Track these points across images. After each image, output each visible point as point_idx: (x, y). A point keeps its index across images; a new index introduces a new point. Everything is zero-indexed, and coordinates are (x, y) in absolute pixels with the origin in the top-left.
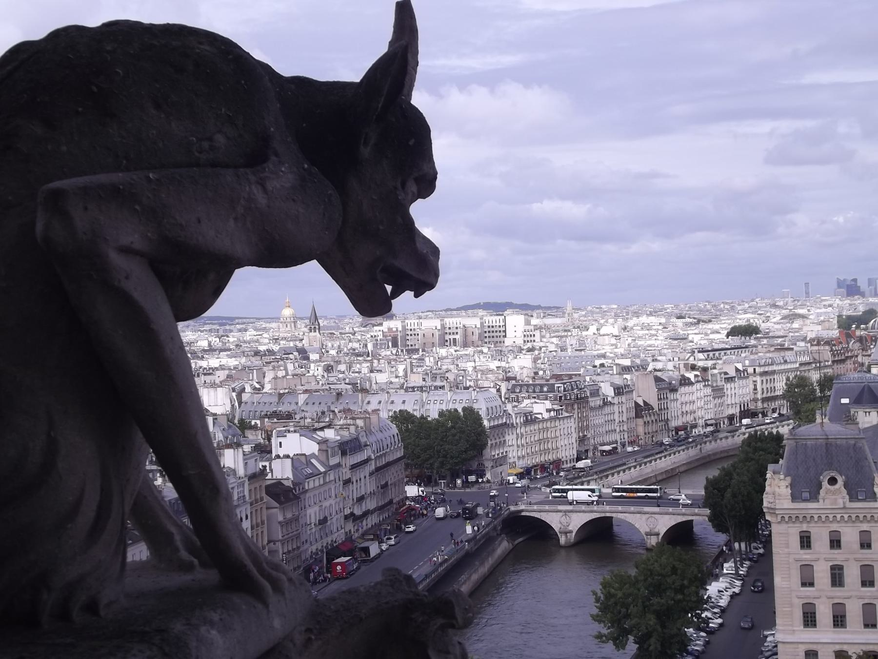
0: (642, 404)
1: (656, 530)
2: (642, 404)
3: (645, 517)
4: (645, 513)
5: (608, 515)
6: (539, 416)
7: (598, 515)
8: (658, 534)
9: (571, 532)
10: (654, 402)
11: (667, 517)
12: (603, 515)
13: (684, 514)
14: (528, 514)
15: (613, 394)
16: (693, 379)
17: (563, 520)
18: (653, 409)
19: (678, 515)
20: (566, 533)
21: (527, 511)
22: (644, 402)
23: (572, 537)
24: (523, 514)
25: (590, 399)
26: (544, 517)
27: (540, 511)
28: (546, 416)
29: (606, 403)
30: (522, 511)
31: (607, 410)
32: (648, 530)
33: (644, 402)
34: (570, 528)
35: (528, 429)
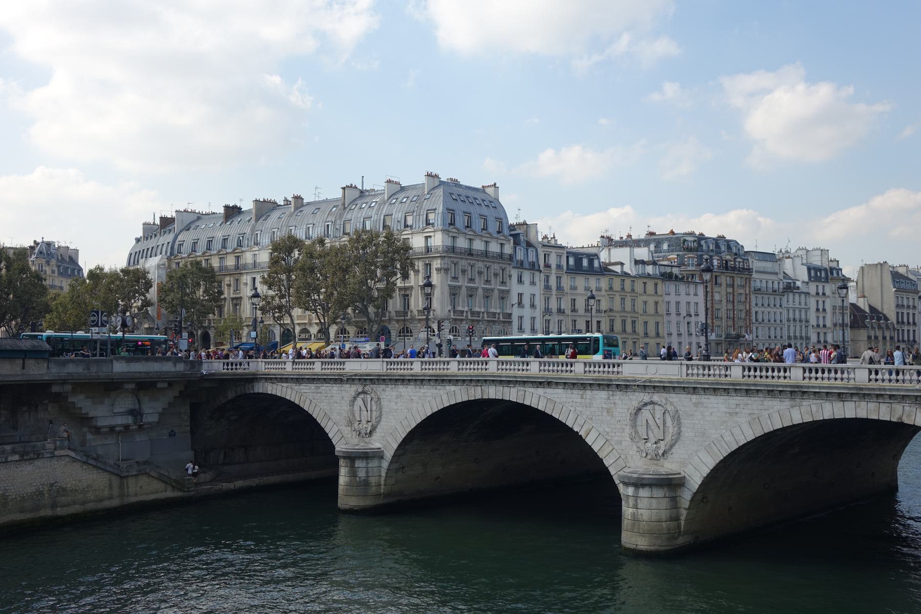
0: (867, 310)
1: (669, 467)
2: (867, 310)
4: (625, 387)
5: (492, 392)
6: (617, 269)
9: (378, 455)
10: (890, 311)
11: (717, 404)
12: (475, 393)
13: (797, 393)
15: (806, 279)
18: (886, 319)
19: (772, 392)
22: (871, 307)
25: (755, 275)
26: (308, 398)
27: (299, 380)
29: (790, 288)
31: (791, 300)
33: (871, 307)
34: (375, 443)
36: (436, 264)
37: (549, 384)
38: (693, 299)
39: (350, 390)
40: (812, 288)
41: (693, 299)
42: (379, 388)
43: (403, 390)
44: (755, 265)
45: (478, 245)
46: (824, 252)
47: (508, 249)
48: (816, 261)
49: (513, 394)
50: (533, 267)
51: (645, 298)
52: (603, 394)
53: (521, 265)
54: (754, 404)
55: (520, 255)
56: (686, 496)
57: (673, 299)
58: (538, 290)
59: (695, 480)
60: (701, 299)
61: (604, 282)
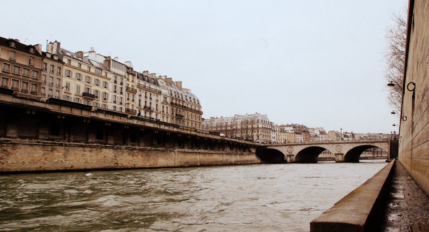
1: (341, 152)
3: (334, 146)
5: (314, 146)
6: (287, 131)
7: (308, 146)
8: (342, 154)
9: (293, 155)
11: (348, 145)
12: (311, 146)
14: (270, 148)
16: (349, 136)
17: (289, 149)
20: (290, 156)
21: (270, 146)
23: (294, 158)
24: (268, 148)
26: (279, 149)
27: (277, 146)
28: (290, 132)
29: (316, 136)
30: (268, 146)
32: (337, 152)
34: (293, 154)
35: (282, 134)
36: (260, 130)
37: (323, 144)
38: (301, 138)
39: (288, 147)
40: (320, 136)
41: (301, 138)
42: (292, 147)
43: (298, 146)
44: (310, 131)
45: (266, 127)
46: (322, 128)
47: (270, 128)
48: (321, 130)
49: (317, 146)
50: (274, 131)
51: (292, 138)
52: (331, 145)
53: (272, 131)
54: (352, 144)
55: (272, 129)
56: (344, 156)
57: (297, 138)
58: (275, 136)
59: (345, 154)
60: (302, 138)
61: (286, 134)
